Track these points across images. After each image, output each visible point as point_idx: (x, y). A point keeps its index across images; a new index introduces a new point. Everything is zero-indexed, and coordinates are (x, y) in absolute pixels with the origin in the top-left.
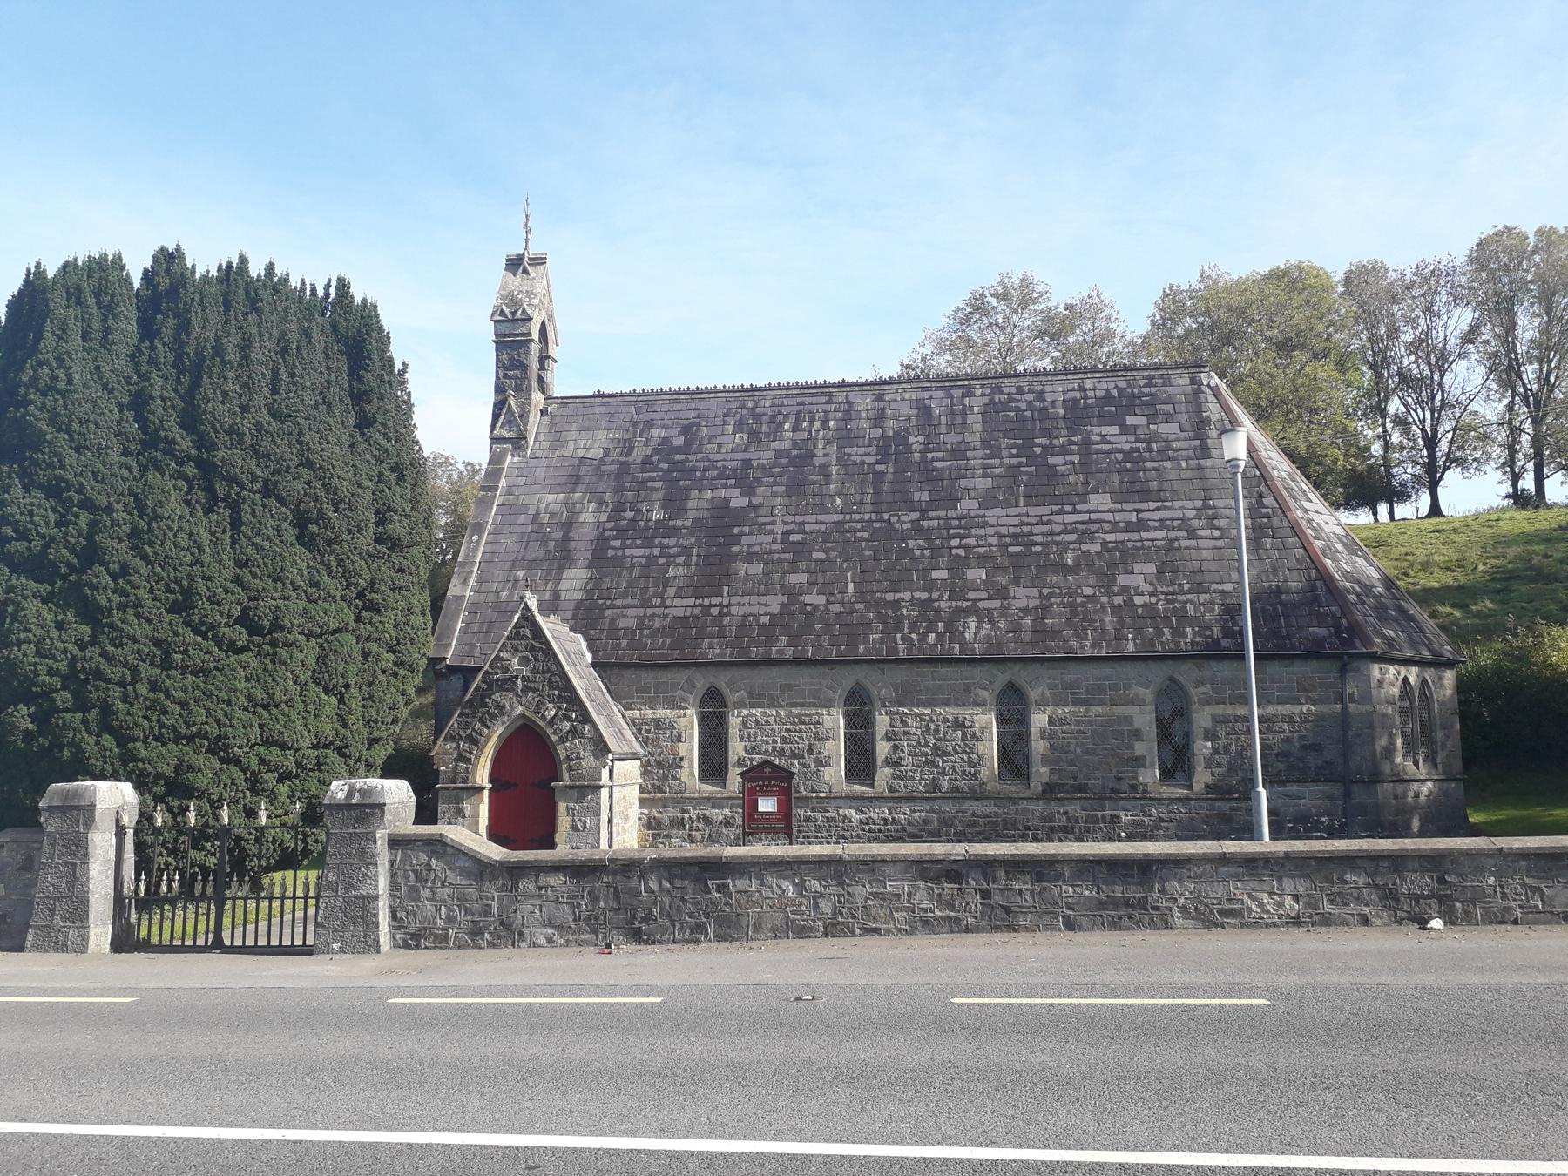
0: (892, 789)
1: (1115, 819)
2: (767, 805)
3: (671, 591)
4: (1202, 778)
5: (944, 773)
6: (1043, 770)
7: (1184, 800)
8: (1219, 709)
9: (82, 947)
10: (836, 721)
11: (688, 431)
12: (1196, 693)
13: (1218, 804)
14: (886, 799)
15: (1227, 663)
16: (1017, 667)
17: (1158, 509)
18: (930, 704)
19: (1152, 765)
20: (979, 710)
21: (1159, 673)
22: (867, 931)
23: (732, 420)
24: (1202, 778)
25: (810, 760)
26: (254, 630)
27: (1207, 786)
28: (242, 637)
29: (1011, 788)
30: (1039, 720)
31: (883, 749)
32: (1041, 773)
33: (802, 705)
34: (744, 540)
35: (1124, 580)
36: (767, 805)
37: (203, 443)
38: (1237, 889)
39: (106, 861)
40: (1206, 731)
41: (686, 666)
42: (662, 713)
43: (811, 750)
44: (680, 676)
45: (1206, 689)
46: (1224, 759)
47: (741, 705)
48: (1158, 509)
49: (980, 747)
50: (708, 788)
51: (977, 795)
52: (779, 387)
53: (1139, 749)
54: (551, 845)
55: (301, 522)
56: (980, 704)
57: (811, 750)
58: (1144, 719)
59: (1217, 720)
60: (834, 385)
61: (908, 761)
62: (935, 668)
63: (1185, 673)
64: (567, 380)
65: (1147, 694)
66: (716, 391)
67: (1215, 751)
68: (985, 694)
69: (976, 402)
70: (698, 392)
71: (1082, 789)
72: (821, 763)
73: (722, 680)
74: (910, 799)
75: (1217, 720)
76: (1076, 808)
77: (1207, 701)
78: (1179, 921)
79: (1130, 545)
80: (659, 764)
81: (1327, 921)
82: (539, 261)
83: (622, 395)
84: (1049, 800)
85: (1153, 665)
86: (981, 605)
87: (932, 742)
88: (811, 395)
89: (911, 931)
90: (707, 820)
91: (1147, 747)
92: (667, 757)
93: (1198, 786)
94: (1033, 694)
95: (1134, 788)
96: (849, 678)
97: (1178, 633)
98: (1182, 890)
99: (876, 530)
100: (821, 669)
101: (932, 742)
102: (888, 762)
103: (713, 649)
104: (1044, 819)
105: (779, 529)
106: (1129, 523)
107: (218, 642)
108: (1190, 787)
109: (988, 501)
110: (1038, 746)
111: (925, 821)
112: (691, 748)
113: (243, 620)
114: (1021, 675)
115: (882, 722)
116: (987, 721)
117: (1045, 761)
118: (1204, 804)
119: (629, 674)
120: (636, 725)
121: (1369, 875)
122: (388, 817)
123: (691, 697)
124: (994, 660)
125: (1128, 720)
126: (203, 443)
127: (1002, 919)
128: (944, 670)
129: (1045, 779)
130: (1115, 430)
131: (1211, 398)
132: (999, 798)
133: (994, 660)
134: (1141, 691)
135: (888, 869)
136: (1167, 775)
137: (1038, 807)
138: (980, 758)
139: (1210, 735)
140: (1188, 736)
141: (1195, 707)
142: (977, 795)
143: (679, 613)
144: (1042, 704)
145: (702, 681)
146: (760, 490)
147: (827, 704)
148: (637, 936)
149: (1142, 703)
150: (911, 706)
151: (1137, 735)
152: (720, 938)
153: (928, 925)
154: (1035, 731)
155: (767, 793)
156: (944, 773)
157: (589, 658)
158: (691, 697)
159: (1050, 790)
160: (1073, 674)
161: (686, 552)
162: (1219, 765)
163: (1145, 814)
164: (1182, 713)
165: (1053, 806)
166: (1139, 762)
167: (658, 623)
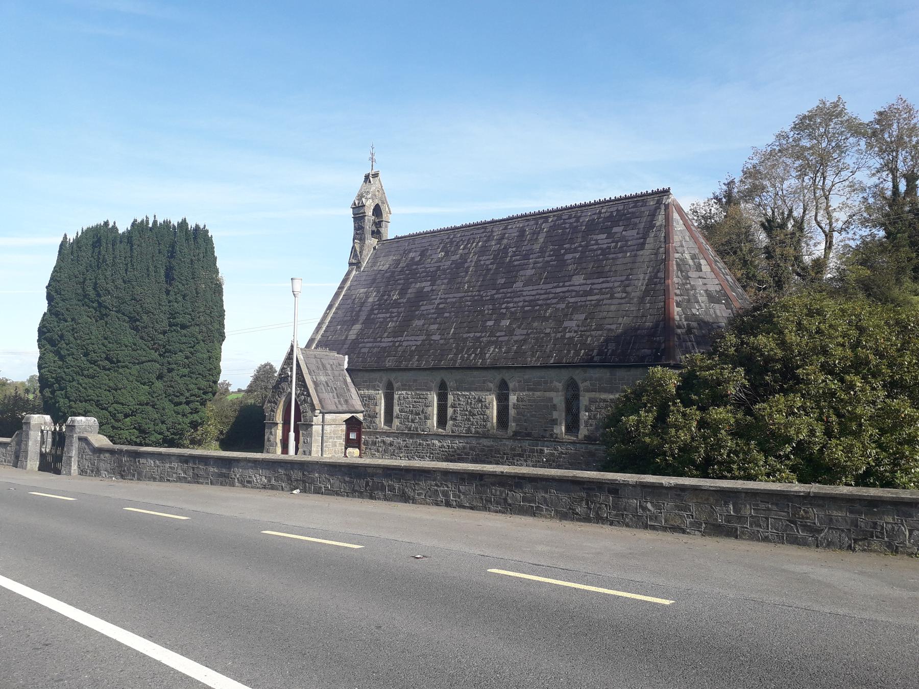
0: (453, 432)
1: (542, 451)
2: (353, 436)
3: (386, 335)
4: (583, 431)
5: (472, 424)
6: (513, 424)
7: (574, 443)
8: (593, 395)
9: (69, 473)
10: (434, 399)
11: (423, 254)
12: (582, 386)
13: (590, 446)
14: (451, 436)
15: (598, 369)
16: (505, 371)
17: (603, 282)
18: (469, 390)
19: (561, 424)
20: (488, 393)
21: (565, 374)
22: (168, 480)
23: (441, 246)
24: (583, 431)
25: (422, 416)
26: (112, 362)
27: (585, 436)
28: (107, 364)
29: (500, 433)
30: (513, 398)
31: (450, 411)
32: (513, 425)
33: (420, 390)
34: (422, 308)
35: (566, 324)
36: (353, 436)
37: (99, 295)
38: (251, 472)
39: (36, 441)
40: (586, 406)
41: (379, 370)
42: (371, 392)
43: (423, 412)
44: (376, 375)
45: (588, 383)
46: (594, 422)
47: (399, 389)
48: (603, 282)
49: (488, 412)
50: (386, 427)
51: (485, 436)
52: (466, 226)
53: (555, 415)
54: (260, 448)
55: (133, 320)
56: (489, 390)
57: (423, 412)
58: (559, 399)
59: (592, 401)
60: (489, 223)
61: (459, 418)
62: (470, 372)
63: (578, 375)
64: (392, 231)
65: (560, 386)
66: (441, 230)
67: (590, 418)
68: (491, 385)
69: (545, 227)
70: (434, 232)
71: (529, 435)
72: (426, 418)
73: (392, 376)
74: (459, 437)
75: (592, 401)
76: (526, 444)
77: (587, 391)
78: (237, 484)
79: (579, 304)
80: (370, 416)
81: (273, 488)
82: (376, 175)
83: (405, 237)
84: (515, 440)
85: (563, 370)
86: (500, 339)
87: (469, 409)
88: (468, 231)
89: (176, 482)
90: (384, 442)
91: (559, 414)
92: (372, 413)
93: (581, 436)
94: (511, 385)
95: (551, 435)
96: (438, 376)
97: (577, 353)
98: (237, 472)
99: (476, 301)
100: (428, 372)
101: (469, 409)
102: (452, 419)
103: (389, 363)
104: (513, 449)
105: (437, 302)
106: (585, 291)
107: (99, 366)
108: (577, 437)
109: (528, 282)
110: (512, 412)
111: (464, 448)
112: (381, 408)
113: (107, 359)
114: (506, 375)
115: (450, 398)
116: (493, 401)
117: (515, 420)
118: (583, 446)
119: (361, 374)
120: (362, 397)
121: (286, 470)
122: (77, 430)
123: (381, 385)
124: (494, 368)
125: (551, 399)
126: (99, 295)
127: (371, 494)
128: (475, 373)
129: (514, 429)
130: (604, 236)
131: (663, 212)
132: (495, 438)
133: (494, 368)
134: (557, 384)
135: (173, 458)
136: (568, 429)
137: (509, 443)
138: (488, 417)
139: (587, 409)
140: (578, 408)
141: (581, 393)
142: (485, 436)
143: (384, 345)
144: (514, 390)
145: (385, 377)
146: (439, 282)
147: (430, 390)
148: (122, 477)
149: (557, 391)
150: (461, 391)
151: (554, 407)
152: (139, 479)
153: (180, 479)
154: (511, 404)
155: (353, 431)
156: (472, 424)
157: (346, 366)
158: (381, 385)
159: (516, 434)
160: (528, 375)
161: (399, 313)
162: (591, 425)
163: (556, 449)
164: (576, 397)
165: (517, 444)
166: (554, 422)
167: (375, 350)
